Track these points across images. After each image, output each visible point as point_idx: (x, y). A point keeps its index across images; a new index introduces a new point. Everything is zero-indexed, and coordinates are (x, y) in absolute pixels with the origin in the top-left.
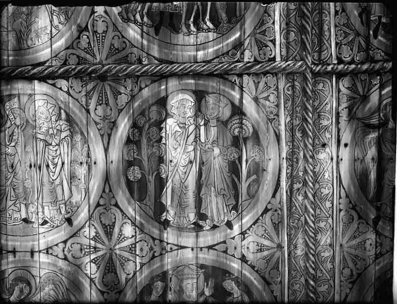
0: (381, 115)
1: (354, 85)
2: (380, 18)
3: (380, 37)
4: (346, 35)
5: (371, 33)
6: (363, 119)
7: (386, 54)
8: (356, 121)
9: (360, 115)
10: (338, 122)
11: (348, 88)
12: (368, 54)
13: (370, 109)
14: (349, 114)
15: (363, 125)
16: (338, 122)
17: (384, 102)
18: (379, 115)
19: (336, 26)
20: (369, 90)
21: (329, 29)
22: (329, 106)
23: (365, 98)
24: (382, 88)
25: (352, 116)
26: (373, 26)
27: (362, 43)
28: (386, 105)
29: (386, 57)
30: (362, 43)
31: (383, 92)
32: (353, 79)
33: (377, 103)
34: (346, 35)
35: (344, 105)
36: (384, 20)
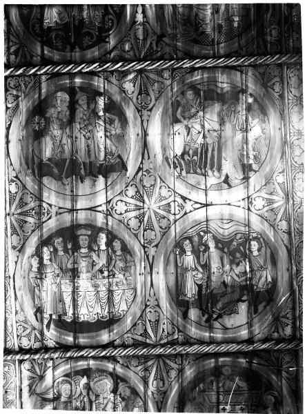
0: (55, 391)
1: (33, 367)
2: (51, 315)
3: (51, 331)
4: (25, 329)
5: (45, 326)
6: (41, 394)
7: (57, 343)
8: (36, 396)
9: (38, 391)
10: (21, 397)
11: (29, 370)
12: (43, 344)
13: (46, 386)
14: (30, 391)
15: (40, 399)
16: (21, 397)
17: (57, 381)
18: (54, 391)
19: (17, 322)
20: (44, 372)
21: (12, 325)
22: (13, 385)
23: (42, 378)
24: (54, 368)
25: (32, 392)
26: (46, 322)
27: (38, 334)
28: (58, 383)
29: (57, 346)
30: (38, 334)
31: (56, 373)
32: (32, 363)
33: (51, 382)
34: (25, 329)
35: (26, 383)
36: (54, 317)
